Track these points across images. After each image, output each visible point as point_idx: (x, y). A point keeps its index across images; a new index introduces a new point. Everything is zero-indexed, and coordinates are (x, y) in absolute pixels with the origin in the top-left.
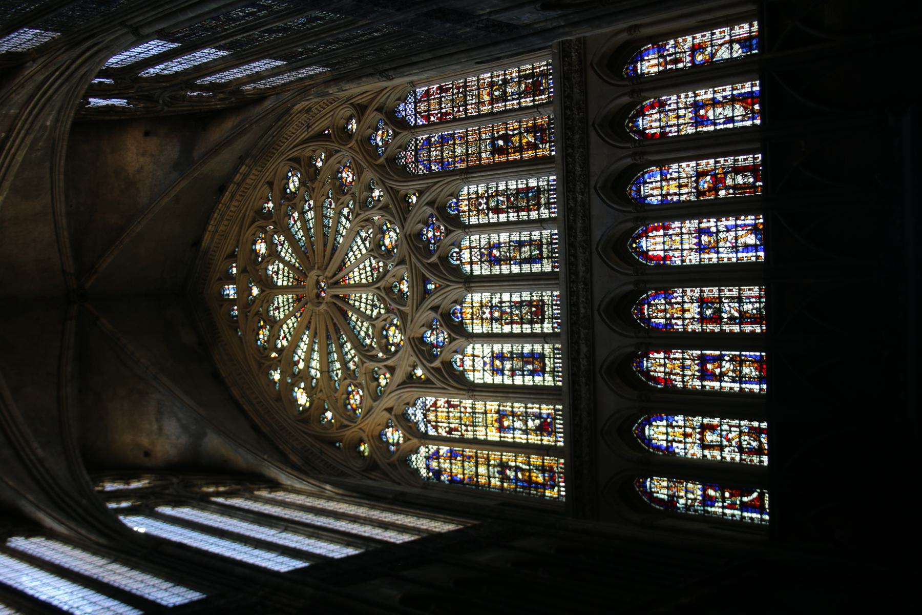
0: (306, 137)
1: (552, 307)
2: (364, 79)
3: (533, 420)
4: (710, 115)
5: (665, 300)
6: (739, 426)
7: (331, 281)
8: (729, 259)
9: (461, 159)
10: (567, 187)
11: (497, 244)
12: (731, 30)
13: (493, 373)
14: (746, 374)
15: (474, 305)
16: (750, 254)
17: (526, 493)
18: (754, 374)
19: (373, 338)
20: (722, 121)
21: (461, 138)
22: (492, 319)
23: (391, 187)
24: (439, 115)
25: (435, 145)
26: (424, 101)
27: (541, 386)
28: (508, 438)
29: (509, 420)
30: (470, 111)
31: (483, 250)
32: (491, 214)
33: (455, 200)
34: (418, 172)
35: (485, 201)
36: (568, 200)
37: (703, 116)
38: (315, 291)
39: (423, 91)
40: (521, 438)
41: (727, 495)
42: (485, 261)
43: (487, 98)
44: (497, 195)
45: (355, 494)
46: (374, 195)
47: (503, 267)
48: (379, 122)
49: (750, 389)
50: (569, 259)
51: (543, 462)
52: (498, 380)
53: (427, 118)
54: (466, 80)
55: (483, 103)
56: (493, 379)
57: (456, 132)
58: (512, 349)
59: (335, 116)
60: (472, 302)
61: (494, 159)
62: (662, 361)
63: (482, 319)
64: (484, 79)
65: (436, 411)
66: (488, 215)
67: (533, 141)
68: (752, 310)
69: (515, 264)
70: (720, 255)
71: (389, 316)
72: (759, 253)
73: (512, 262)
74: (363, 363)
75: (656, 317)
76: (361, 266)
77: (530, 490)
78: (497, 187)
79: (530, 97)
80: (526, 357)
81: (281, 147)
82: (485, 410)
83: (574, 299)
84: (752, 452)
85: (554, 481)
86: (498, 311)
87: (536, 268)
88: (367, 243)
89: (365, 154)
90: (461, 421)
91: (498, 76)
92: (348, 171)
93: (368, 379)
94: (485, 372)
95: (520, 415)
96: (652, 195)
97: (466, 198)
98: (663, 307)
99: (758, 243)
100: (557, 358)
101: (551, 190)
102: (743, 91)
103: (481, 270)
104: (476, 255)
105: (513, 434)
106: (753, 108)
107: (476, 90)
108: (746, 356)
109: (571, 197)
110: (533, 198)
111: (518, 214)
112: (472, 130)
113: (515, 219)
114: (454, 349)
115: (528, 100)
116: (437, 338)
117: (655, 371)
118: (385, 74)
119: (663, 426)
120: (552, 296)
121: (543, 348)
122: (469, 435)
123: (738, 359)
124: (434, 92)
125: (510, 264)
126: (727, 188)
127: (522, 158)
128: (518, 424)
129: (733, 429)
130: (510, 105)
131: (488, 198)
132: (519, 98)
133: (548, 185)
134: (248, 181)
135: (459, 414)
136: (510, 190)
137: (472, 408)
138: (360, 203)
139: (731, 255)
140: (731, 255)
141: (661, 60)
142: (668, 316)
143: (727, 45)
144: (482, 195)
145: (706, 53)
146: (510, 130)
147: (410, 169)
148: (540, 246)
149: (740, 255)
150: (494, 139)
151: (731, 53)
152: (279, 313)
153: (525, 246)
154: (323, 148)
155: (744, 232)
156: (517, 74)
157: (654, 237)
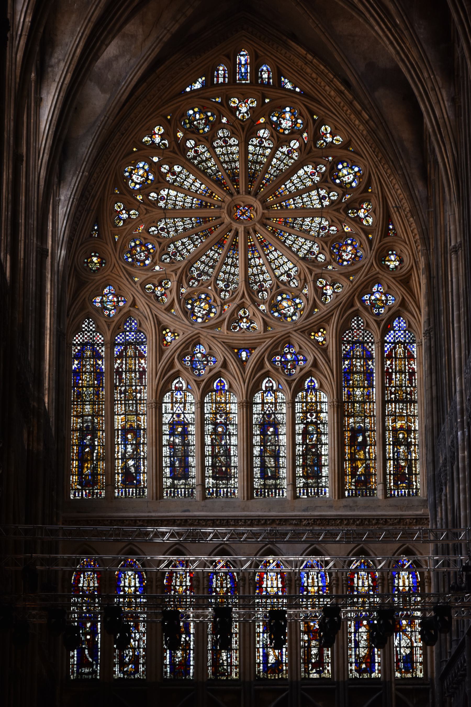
0: (389, 201)
1: (225, 488)
2: (427, 309)
3: (133, 465)
4: (362, 629)
5: (230, 587)
6: (139, 647)
7: (251, 231)
8: (259, 642)
9: (351, 394)
10: (318, 519)
11: (278, 431)
12: (420, 647)
13: (169, 424)
14: (177, 654)
15: (228, 406)
16: (261, 658)
17: (73, 456)
18: (177, 660)
19: (199, 281)
20: (357, 639)
21: (368, 395)
22: (216, 425)
23: (333, 314)
24: (390, 371)
25: (366, 365)
26: (404, 353)
27: (163, 474)
28: (118, 438)
29: (133, 440)
30: (390, 406)
31: (273, 416)
32: (302, 426)
33: (317, 386)
34: (344, 344)
35: (314, 420)
36: (308, 519)
37: (362, 623)
38: (242, 204)
39: (413, 351)
40: (118, 452)
41: (88, 637)
42: (264, 419)
43: (398, 425)
44: (317, 433)
45: (60, 286)
46: (328, 287)
47: (258, 438)
48: (393, 296)
49: (166, 657)
50: (263, 520)
51: (100, 475)
52: (166, 428)
53: (389, 357)
54: (416, 402)
55: (394, 421)
56: (166, 424)
57: (374, 389)
58: (192, 446)
59: (404, 244)
60: (231, 403)
61: (348, 431)
62: (184, 584)
63: (216, 414)
64: (414, 422)
65: (135, 356)
66: (302, 423)
67: (358, 473)
68: (222, 660)
69: (261, 451)
70: (261, 634)
71: (218, 306)
72: (261, 665)
73: (262, 448)
74: (175, 271)
75: (217, 579)
76: (264, 268)
77: (76, 460)
78: (325, 434)
79: (393, 471)
80: (185, 460)
81: (382, 166)
82: (139, 414)
83: (232, 523)
84: (122, 658)
85: (86, 486)
86: (222, 431)
87: (257, 471)
88: (284, 278)
89: (365, 283)
90: (128, 386)
91: (415, 438)
92: (352, 254)
93: (161, 276)
94: (171, 415)
95: (137, 452)
96: (308, 578)
97: (318, 400)
98: (224, 585)
99: (269, 665)
100: (185, 491)
101: (318, 490)
102: (376, 656)
103: (257, 414)
104: (269, 409)
105: (121, 444)
106: (363, 663)
107: (407, 413)
108: (190, 654)
109: (310, 522)
110: (313, 471)
111: (301, 455)
112: (373, 408)
113: (297, 453)
114: (190, 383)
115: (392, 469)
116: (199, 361)
117: (176, 577)
118: (427, 333)
119: (135, 584)
120: (234, 488)
121: (193, 478)
122: (117, 396)
123: (187, 648)
124: (411, 365)
125: (260, 446)
126: (309, 641)
127: (346, 460)
128: (129, 449)
129: (137, 643)
130: (389, 448)
131: (316, 424)
132: (394, 459)
133: (322, 487)
134: (353, 116)
135: (134, 384)
136: (321, 447)
137: (140, 400)
139: (261, 643)
140: (261, 643)
141: (407, 588)
142: (218, 589)
143: (410, 645)
144: (319, 417)
145: (407, 627)
146: (369, 449)
147: (347, 334)
148: (275, 476)
149: (261, 650)
150: (363, 431)
151: (404, 647)
152: (222, 147)
153: (275, 462)
154: (376, 226)
155: (277, 654)
156: (413, 458)
157: (276, 579)
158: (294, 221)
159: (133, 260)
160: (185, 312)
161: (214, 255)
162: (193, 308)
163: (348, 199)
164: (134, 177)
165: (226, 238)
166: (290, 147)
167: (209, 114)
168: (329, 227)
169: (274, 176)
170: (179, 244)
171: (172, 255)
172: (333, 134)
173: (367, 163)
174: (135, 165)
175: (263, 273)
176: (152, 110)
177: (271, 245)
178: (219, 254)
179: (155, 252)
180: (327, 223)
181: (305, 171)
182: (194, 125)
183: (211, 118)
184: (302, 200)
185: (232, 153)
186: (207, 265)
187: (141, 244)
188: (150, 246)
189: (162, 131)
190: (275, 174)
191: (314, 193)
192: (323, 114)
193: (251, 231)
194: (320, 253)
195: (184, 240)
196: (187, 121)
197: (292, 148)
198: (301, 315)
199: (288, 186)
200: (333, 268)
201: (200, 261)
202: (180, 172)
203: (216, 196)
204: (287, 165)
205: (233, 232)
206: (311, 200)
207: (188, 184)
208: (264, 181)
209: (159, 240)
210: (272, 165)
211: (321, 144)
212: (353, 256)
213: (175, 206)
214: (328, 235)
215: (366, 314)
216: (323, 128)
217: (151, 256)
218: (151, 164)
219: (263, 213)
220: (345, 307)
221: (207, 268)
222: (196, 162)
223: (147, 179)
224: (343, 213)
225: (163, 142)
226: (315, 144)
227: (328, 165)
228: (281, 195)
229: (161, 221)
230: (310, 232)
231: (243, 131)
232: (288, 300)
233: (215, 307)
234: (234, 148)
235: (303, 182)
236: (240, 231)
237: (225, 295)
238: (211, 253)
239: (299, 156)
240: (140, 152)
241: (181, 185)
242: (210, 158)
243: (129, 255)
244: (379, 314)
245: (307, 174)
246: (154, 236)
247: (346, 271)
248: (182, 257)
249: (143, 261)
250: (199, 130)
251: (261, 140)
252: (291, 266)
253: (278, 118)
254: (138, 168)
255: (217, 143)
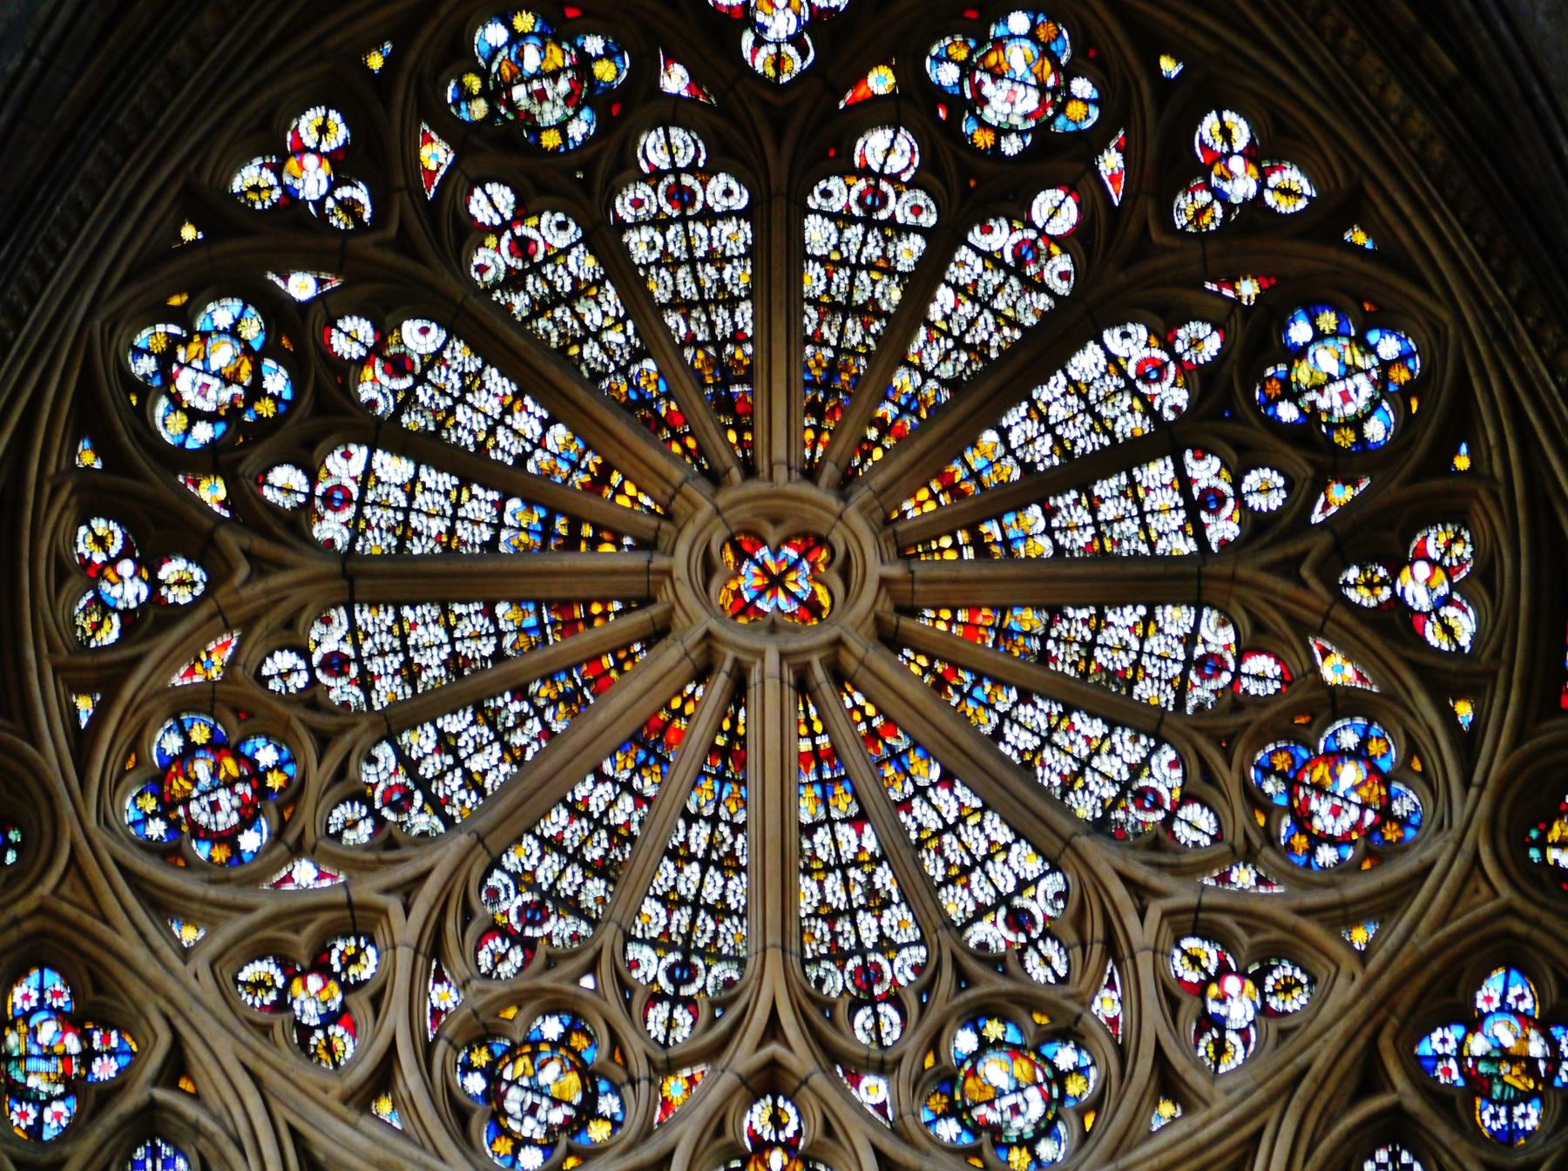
7: (819, 673)
19: (529, 945)
23: (1257, 1137)
46: (1232, 984)
71: (633, 1082)
76: (884, 877)
81: (1532, 334)
88: (992, 932)
89: (1435, 966)
92: (1363, 807)
93: (324, 917)
134: (1371, 63)
138: (1199, 908)
152: (661, 223)
154: (1497, 654)
158: (1049, 625)
159: (173, 826)
160: (459, 1113)
161: (612, 804)
162: (493, 1094)
163: (1345, 509)
164: (185, 382)
165: (679, 713)
166: (1030, 224)
167: (594, 45)
168: (1239, 660)
169: (943, 383)
170: (421, 741)
171: (387, 802)
172: (1261, 156)
173: (1446, 316)
174: (184, 317)
175: (877, 903)
176: (284, 20)
177: (928, 755)
178: (640, 798)
179: (294, 792)
180: (1228, 635)
181: (1111, 358)
182: (512, 105)
183: (605, 71)
184: (1093, 511)
185: (717, 259)
186: (576, 857)
187: (216, 746)
188: (267, 756)
189: (339, 134)
190: (946, 371)
191: (1158, 472)
192: (1213, 49)
193: (819, 673)
194: (1187, 798)
195: (451, 724)
196: (474, 83)
197: (1041, 232)
198: (1085, 1136)
199: (1015, 438)
200: (1260, 880)
201: (541, 839)
202: (437, 356)
203: (630, 489)
204: (1013, 324)
205: (720, 681)
206: (1142, 515)
207: (479, 424)
208: (888, 410)
209: (318, 719)
210: (931, 325)
211: (1200, 213)
212: (1370, 817)
213: (402, 540)
214: (1233, 700)
215: (1443, 1132)
216: (1210, 123)
217: (271, 808)
218: (276, 310)
219: (884, 581)
220: (1324, 1096)
221: (574, 874)
222: (519, 303)
223: (256, 391)
224: (1313, 583)
225: (344, 192)
226: (1166, 211)
227: (1236, 325)
228: (980, 484)
229: (327, 621)
230: (1134, 681)
231: (778, 139)
232: (1016, 1051)
233: (615, 1089)
234: (728, 228)
235: (1098, 417)
236: (754, 677)
237: (670, 1024)
238: (598, 796)
239: (1083, 276)
240: (217, 249)
241: (440, 426)
242: (598, 284)
243: (150, 804)
244: (1510, 1134)
245: (1122, 373)
246: (287, 698)
247: (1330, 896)
248: (439, 812)
249: (229, 839)
250: (537, 130)
251: (875, 190)
252: (1031, 865)
253: (967, 68)
254: (205, 336)
255: (638, 204)
